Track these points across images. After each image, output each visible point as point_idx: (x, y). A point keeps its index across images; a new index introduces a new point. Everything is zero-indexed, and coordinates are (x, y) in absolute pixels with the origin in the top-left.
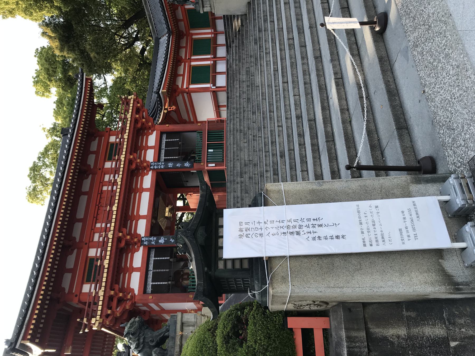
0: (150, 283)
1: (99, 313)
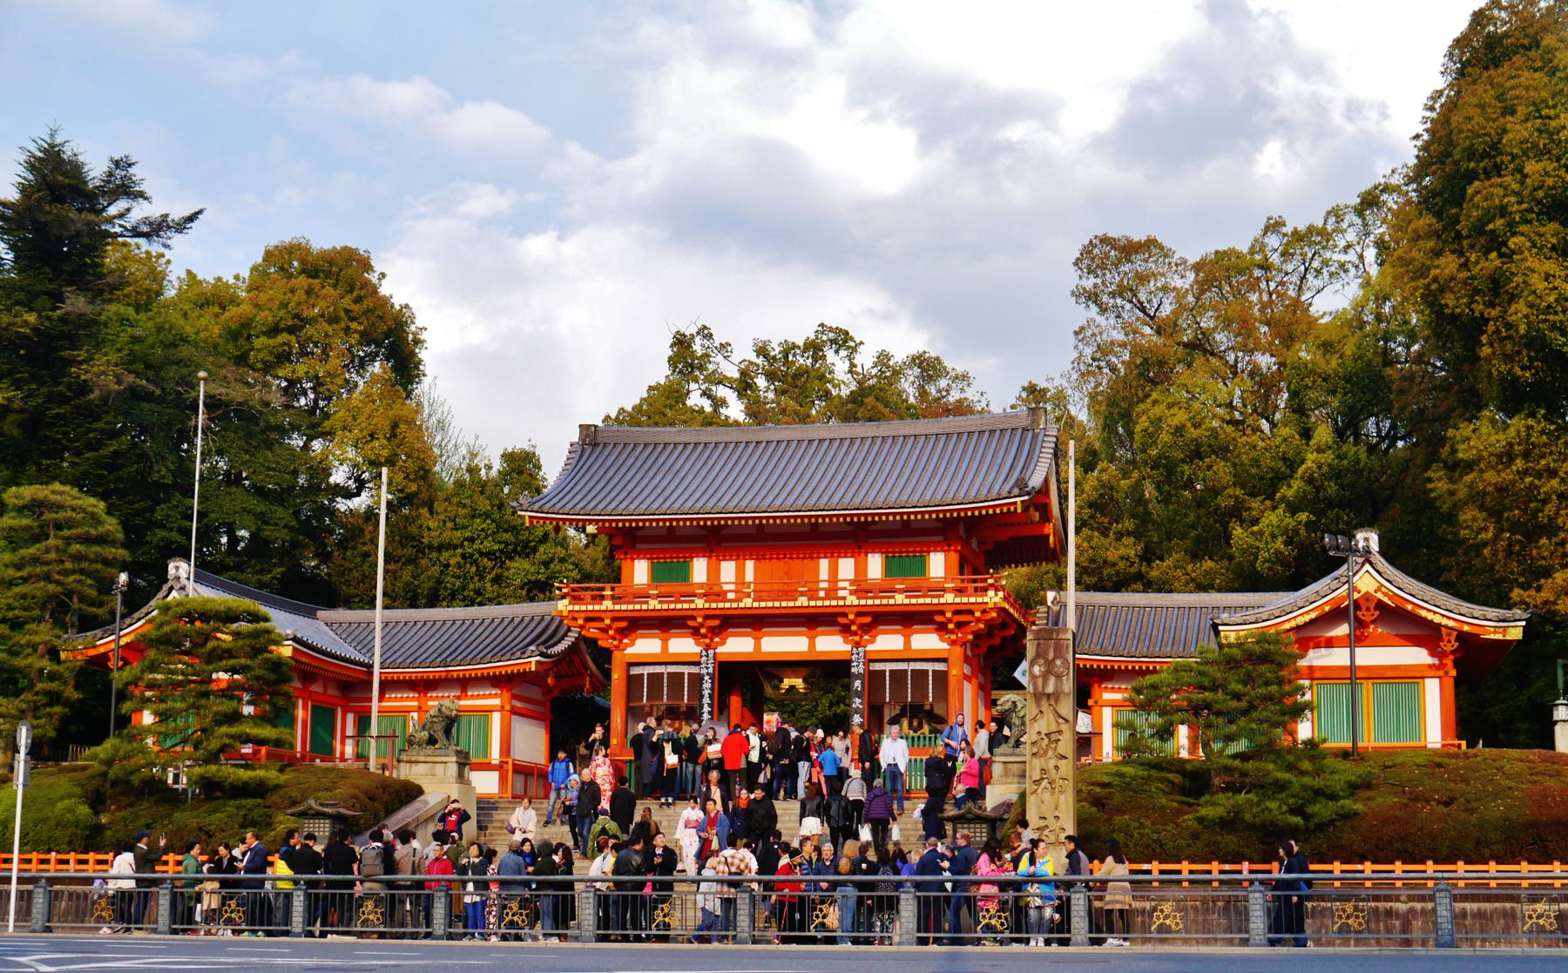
0: (646, 670)
1: (577, 608)
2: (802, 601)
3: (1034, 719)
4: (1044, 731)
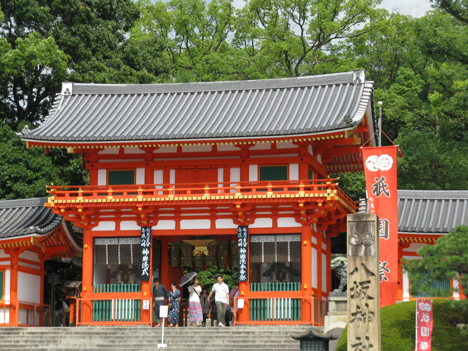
0: (107, 242)
1: (60, 201)
2: (206, 196)
3: (352, 273)
4: (358, 281)
